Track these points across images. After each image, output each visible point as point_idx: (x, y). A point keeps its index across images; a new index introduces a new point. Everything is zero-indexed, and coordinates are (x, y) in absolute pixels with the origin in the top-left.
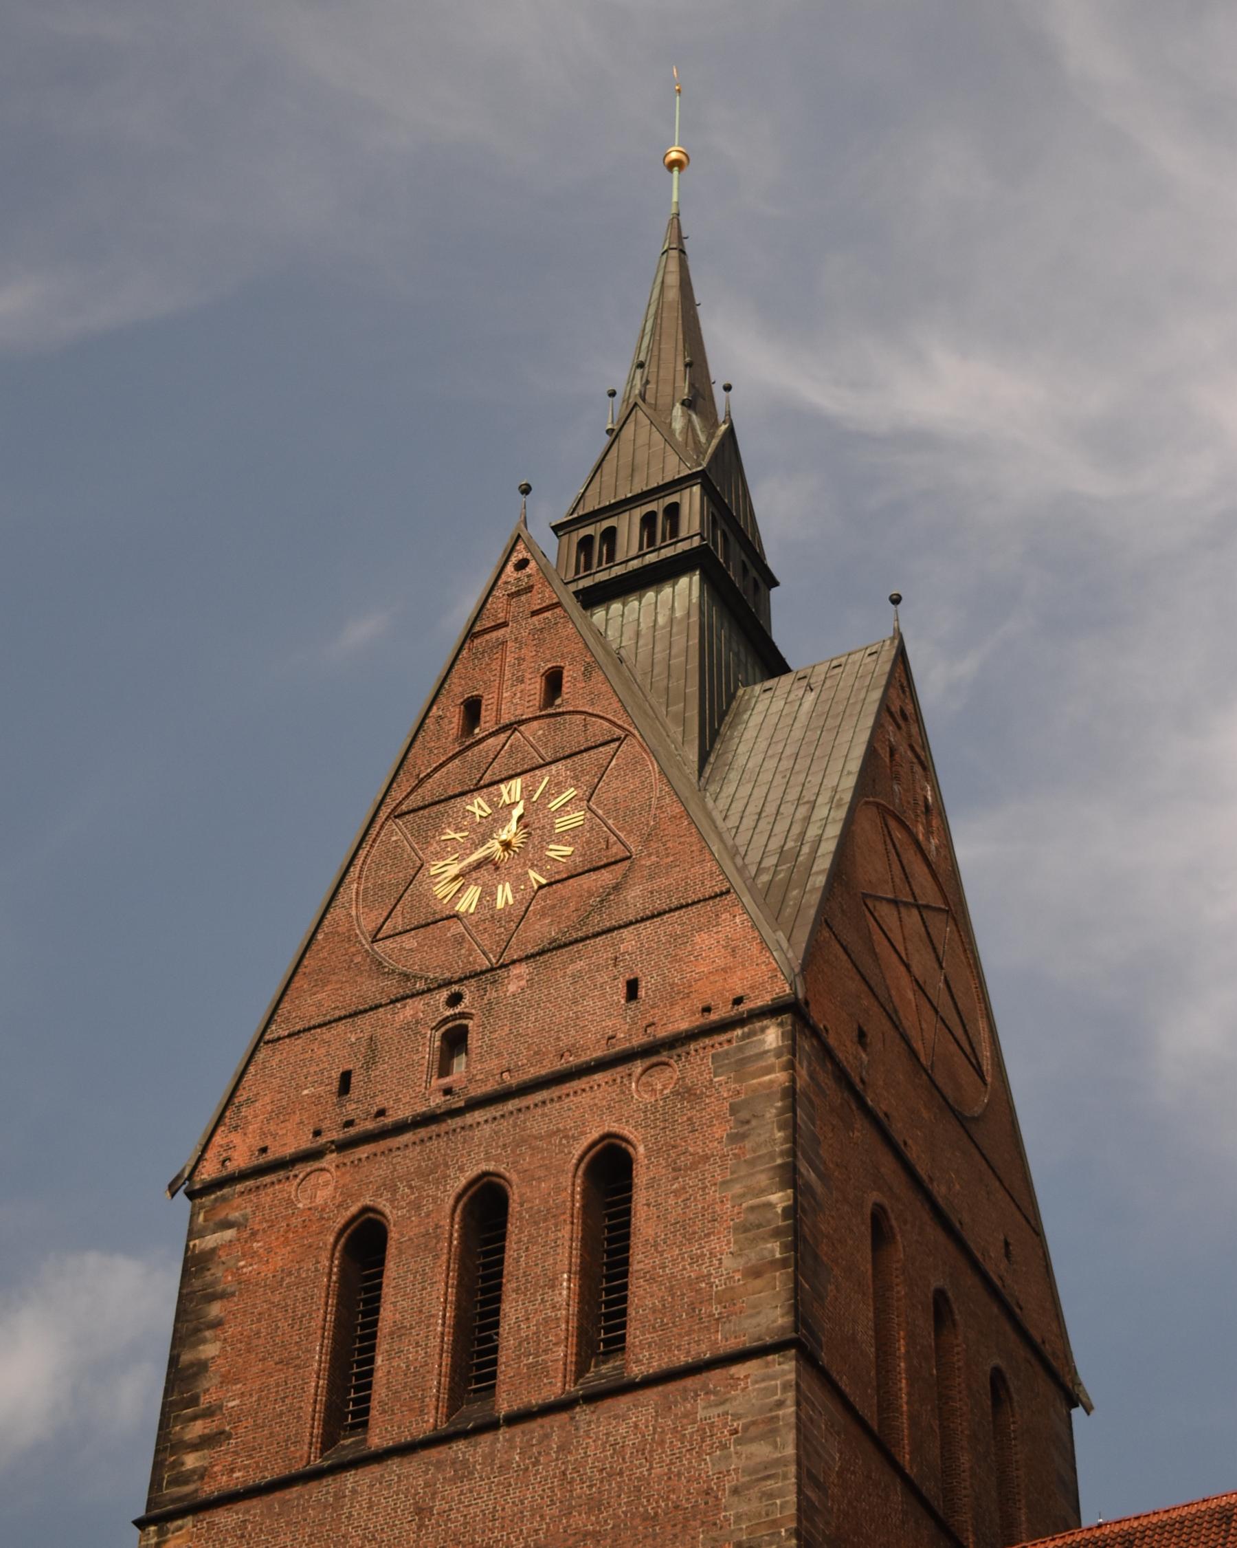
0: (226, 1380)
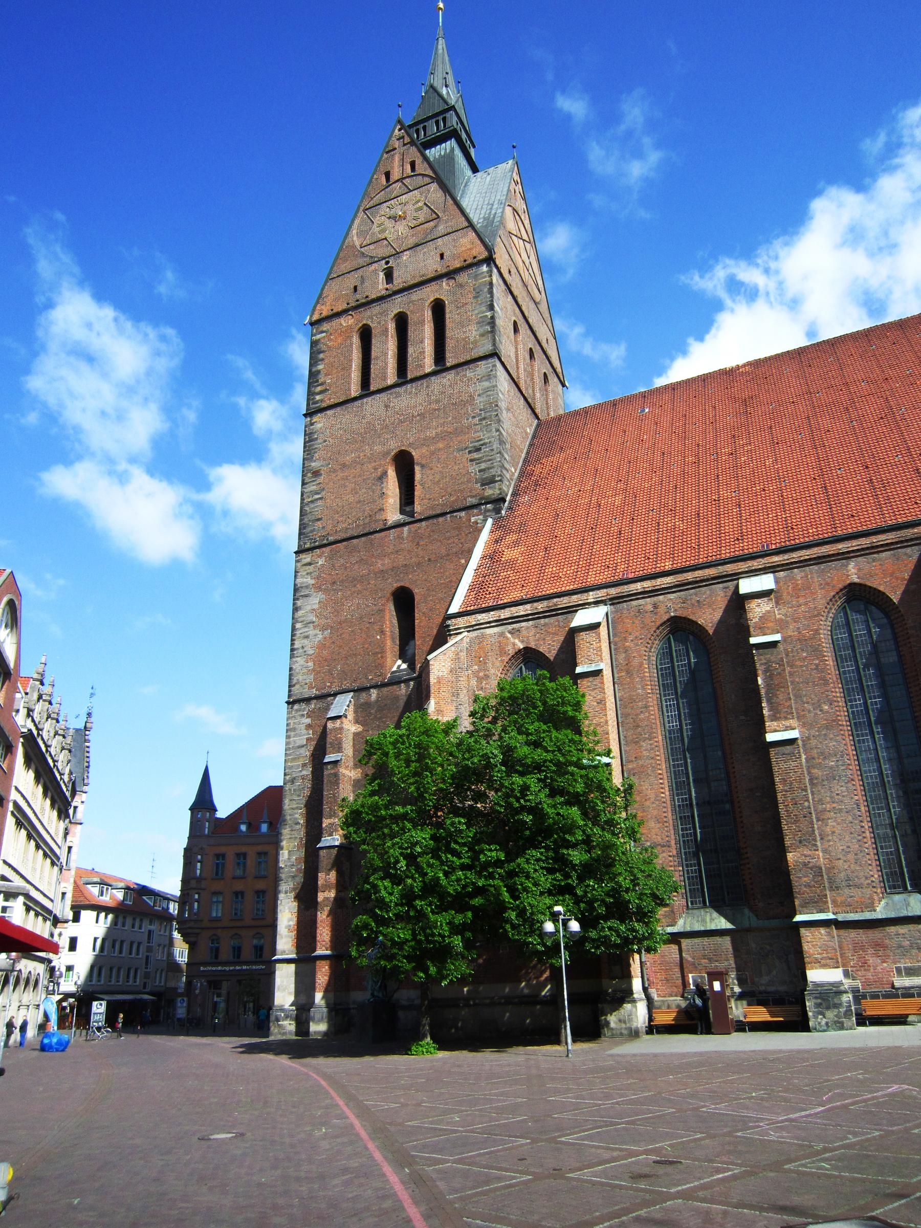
0: (326, 375)
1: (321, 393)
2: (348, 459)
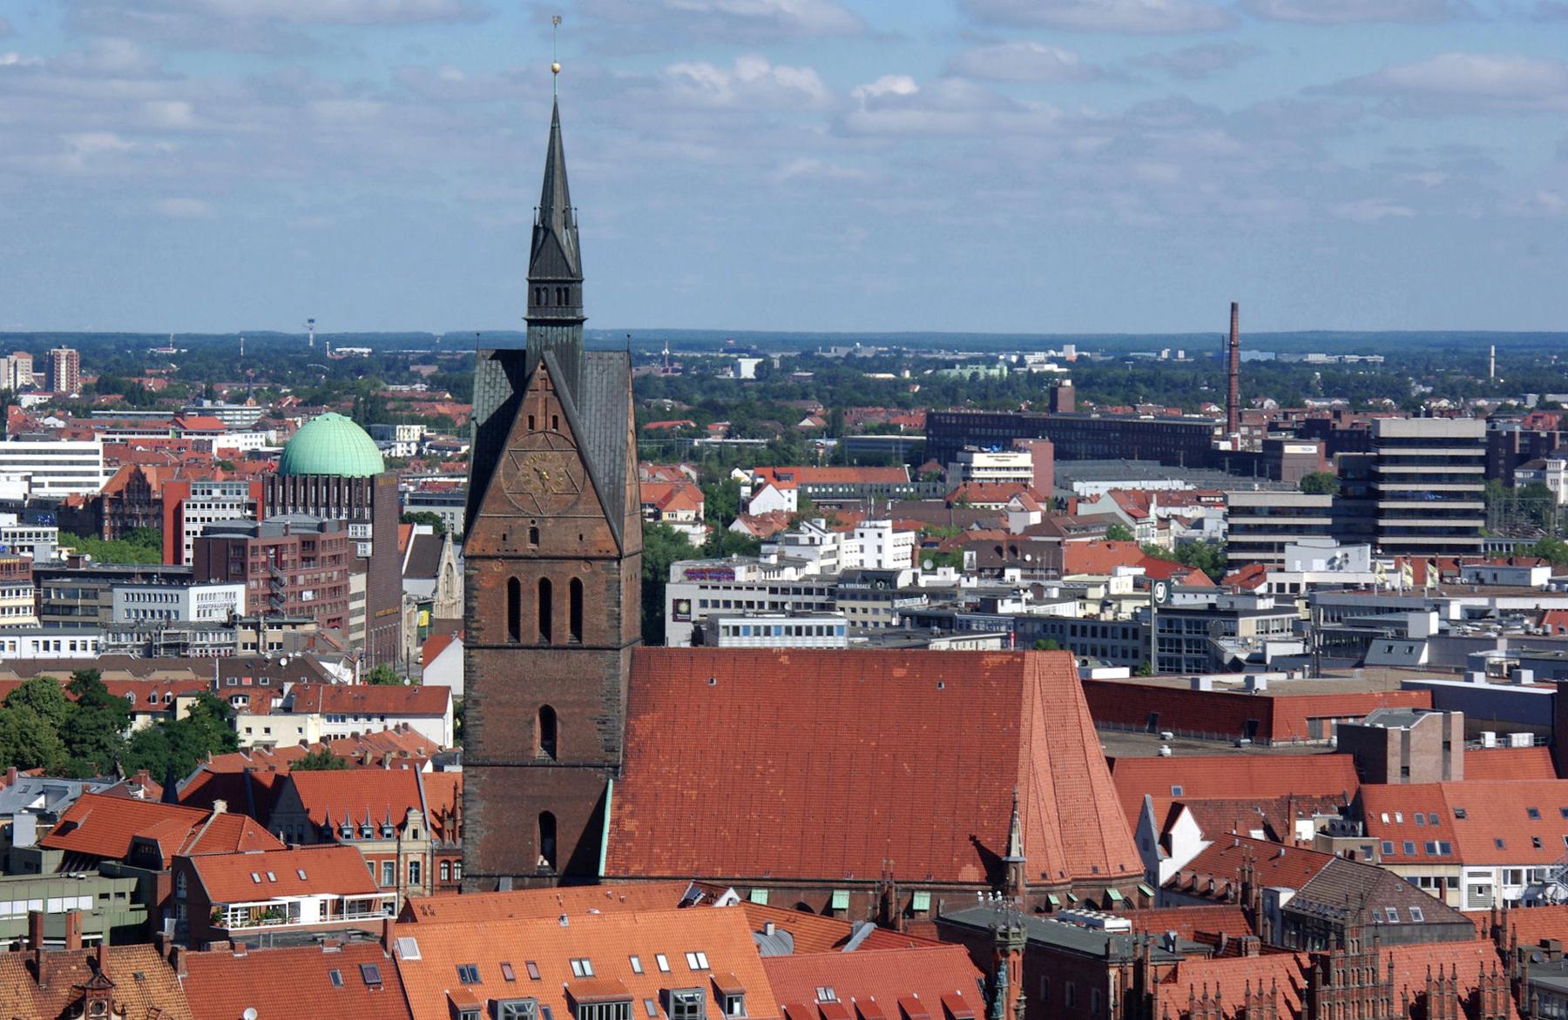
1: (477, 629)
2: (504, 698)
